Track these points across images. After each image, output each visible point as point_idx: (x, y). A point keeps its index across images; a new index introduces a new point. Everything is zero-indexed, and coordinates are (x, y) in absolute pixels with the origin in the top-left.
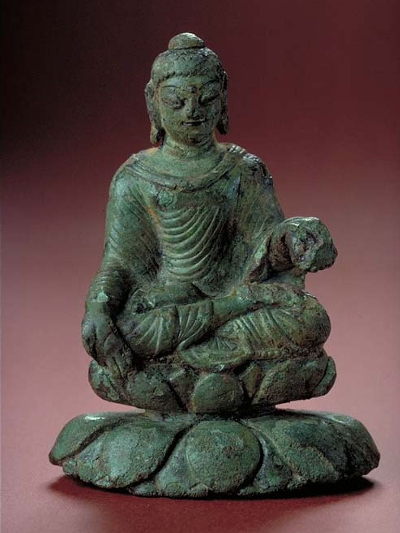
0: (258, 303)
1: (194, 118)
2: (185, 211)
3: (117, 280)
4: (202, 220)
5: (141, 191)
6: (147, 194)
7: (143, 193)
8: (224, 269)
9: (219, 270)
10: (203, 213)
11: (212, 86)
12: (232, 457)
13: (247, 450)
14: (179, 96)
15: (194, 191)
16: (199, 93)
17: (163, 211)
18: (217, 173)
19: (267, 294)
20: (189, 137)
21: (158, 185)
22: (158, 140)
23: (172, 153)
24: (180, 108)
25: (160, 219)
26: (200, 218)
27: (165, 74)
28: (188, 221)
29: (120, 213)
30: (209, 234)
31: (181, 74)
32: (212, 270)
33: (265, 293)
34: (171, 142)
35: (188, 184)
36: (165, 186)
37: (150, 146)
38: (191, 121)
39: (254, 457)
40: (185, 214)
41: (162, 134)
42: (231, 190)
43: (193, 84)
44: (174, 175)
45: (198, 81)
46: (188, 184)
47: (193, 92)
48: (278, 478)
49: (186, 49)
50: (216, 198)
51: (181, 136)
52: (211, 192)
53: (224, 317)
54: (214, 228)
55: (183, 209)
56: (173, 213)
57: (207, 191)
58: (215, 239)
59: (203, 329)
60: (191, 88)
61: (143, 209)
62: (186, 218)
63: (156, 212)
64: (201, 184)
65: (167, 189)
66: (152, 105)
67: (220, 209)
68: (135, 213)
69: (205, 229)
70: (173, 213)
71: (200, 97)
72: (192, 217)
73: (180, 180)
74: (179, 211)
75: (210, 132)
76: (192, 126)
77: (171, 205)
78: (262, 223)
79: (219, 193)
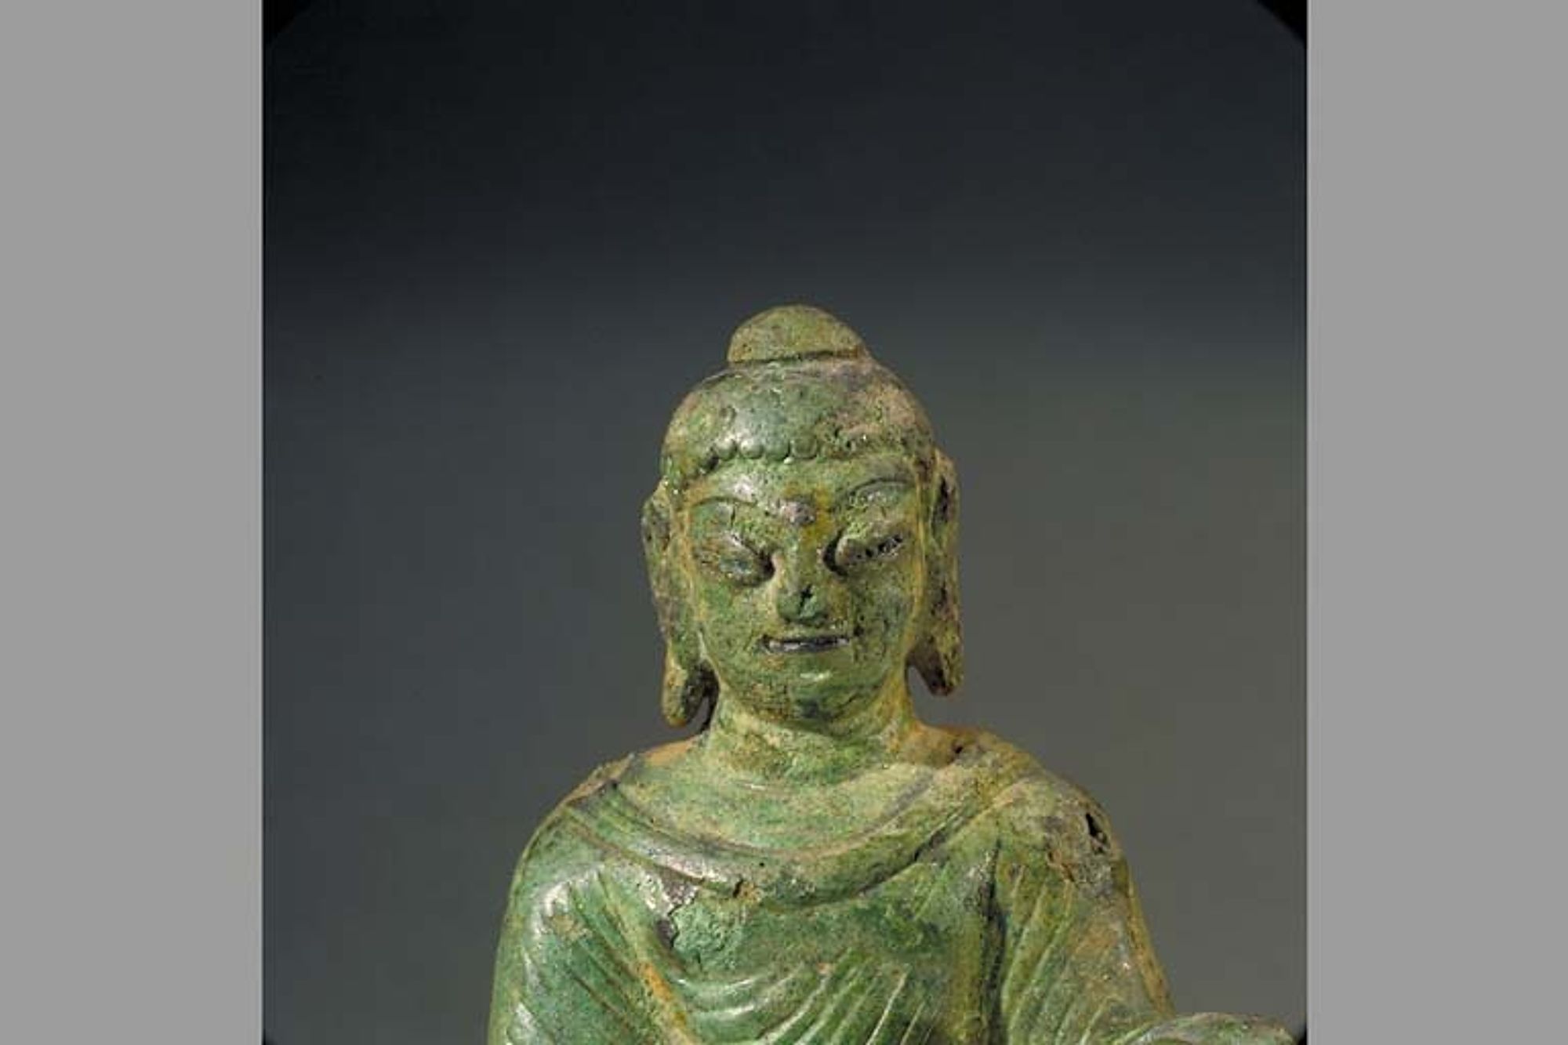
1: (806, 622)
2: (773, 979)
5: (612, 901)
6: (633, 911)
7: (621, 909)
10: (844, 990)
11: (881, 496)
14: (752, 536)
15: (809, 900)
16: (829, 523)
17: (692, 978)
18: (901, 838)
20: (791, 695)
21: (674, 880)
22: (690, 709)
23: (742, 761)
24: (757, 582)
25: (684, 1008)
26: (830, 1009)
27: (703, 451)
28: (782, 1020)
29: (533, 979)
31: (759, 453)
34: (735, 717)
35: (786, 876)
36: (701, 882)
37: (662, 734)
38: (796, 632)
40: (773, 993)
41: (704, 687)
42: (956, 901)
43: (806, 490)
45: (826, 478)
46: (786, 876)
47: (805, 522)
49: (785, 360)
50: (898, 935)
51: (763, 691)
52: (874, 908)
55: (764, 974)
56: (730, 989)
57: (861, 903)
60: (794, 505)
61: (622, 969)
62: (776, 1005)
63: (668, 983)
64: (836, 879)
65: (707, 893)
66: (668, 572)
67: (910, 979)
68: (591, 982)
70: (730, 989)
71: (833, 545)
72: (799, 1002)
73: (756, 863)
75: (874, 680)
76: (800, 651)
77: (720, 956)
78: (1081, 1033)
79: (910, 916)
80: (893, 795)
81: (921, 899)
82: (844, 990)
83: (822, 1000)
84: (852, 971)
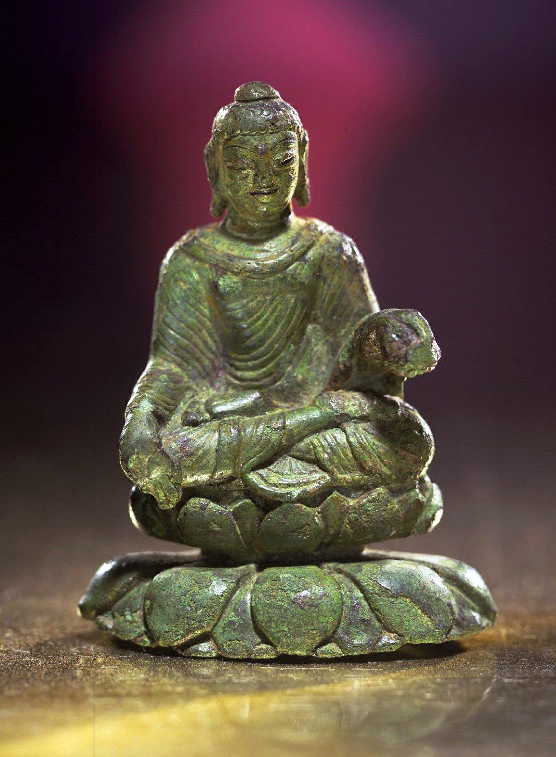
0: (342, 415)
2: (252, 301)
3: (166, 386)
4: (272, 313)
8: (301, 374)
9: (295, 375)
12: (307, 607)
13: (325, 600)
19: (353, 405)
26: (270, 309)
30: (282, 329)
32: (286, 375)
33: (351, 403)
39: (335, 609)
44: (239, 255)
48: (364, 635)
50: (292, 286)
53: (299, 433)
54: (289, 322)
57: (280, 275)
58: (290, 336)
59: (272, 447)
69: (276, 323)
72: (261, 308)
74: (245, 301)
80: (290, 240)
81: (299, 274)
82: (275, 304)
83: (267, 307)
84: (277, 297)
